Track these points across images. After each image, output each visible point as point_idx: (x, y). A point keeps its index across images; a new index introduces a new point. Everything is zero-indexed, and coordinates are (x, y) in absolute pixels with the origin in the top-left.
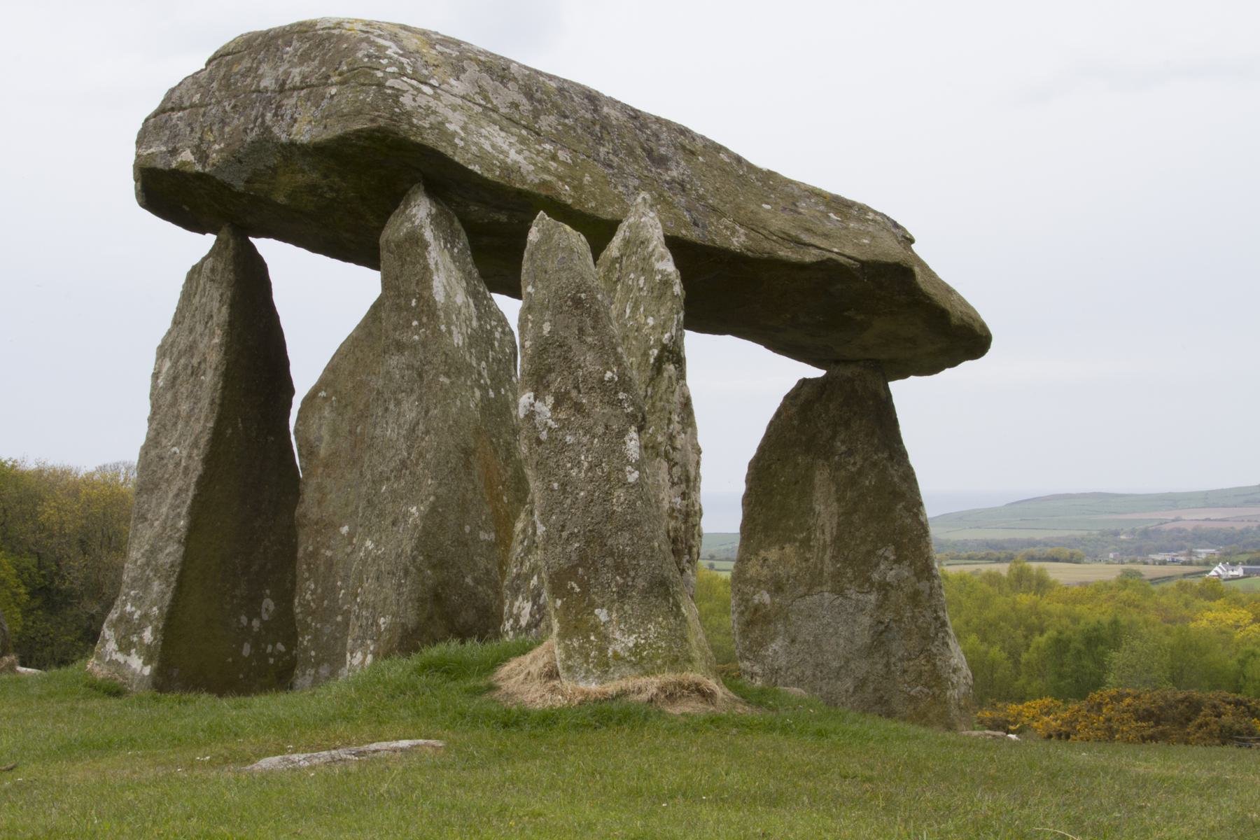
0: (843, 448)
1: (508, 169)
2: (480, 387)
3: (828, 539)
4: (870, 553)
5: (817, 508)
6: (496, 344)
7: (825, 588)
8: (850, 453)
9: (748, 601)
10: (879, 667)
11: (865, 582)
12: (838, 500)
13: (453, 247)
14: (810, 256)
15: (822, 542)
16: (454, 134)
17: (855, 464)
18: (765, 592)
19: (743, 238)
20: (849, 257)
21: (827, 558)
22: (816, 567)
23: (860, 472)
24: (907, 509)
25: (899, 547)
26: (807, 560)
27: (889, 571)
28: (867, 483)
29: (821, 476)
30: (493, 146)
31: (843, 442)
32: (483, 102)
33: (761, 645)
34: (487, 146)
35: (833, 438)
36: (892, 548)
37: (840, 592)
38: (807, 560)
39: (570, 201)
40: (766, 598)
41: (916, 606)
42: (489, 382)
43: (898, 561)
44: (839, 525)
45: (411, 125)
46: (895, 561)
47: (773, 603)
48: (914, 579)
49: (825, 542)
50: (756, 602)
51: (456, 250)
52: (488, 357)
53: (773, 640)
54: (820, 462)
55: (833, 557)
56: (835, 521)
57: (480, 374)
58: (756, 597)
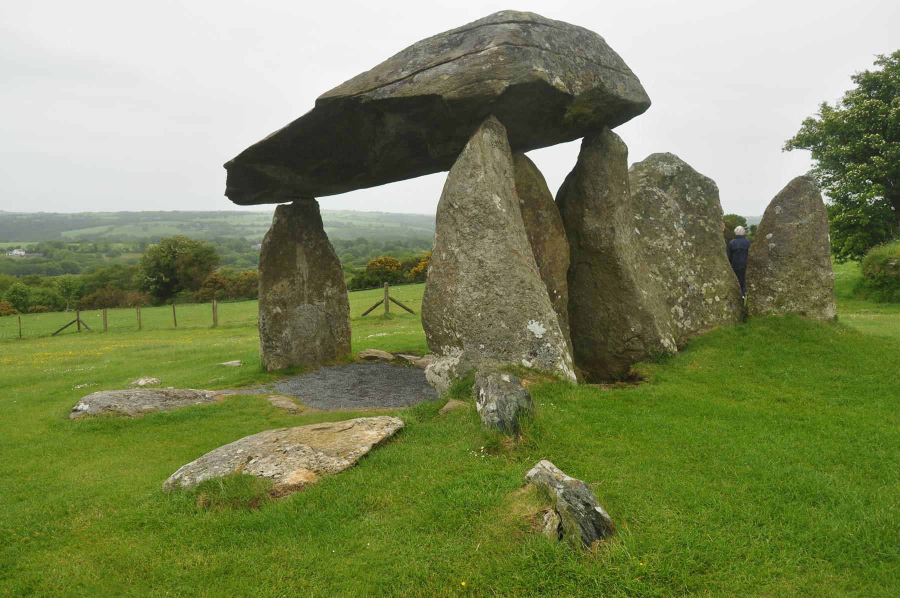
0: (306, 238)
3: (306, 280)
4: (324, 284)
5: (298, 266)
7: (305, 302)
8: (309, 240)
9: (270, 313)
10: (328, 332)
11: (321, 297)
12: (308, 261)
15: (301, 281)
17: (312, 245)
18: (278, 308)
21: (305, 288)
22: (300, 293)
23: (314, 248)
24: (336, 263)
25: (333, 280)
26: (295, 290)
27: (329, 291)
28: (318, 253)
29: (300, 250)
31: (306, 235)
33: (281, 333)
35: (301, 233)
36: (330, 281)
37: (311, 302)
38: (295, 290)
40: (279, 310)
41: (340, 304)
43: (332, 286)
44: (309, 272)
46: (332, 287)
47: (283, 312)
48: (339, 293)
49: (303, 280)
50: (275, 312)
53: (285, 330)
54: (298, 244)
55: (308, 287)
56: (307, 271)
58: (274, 310)
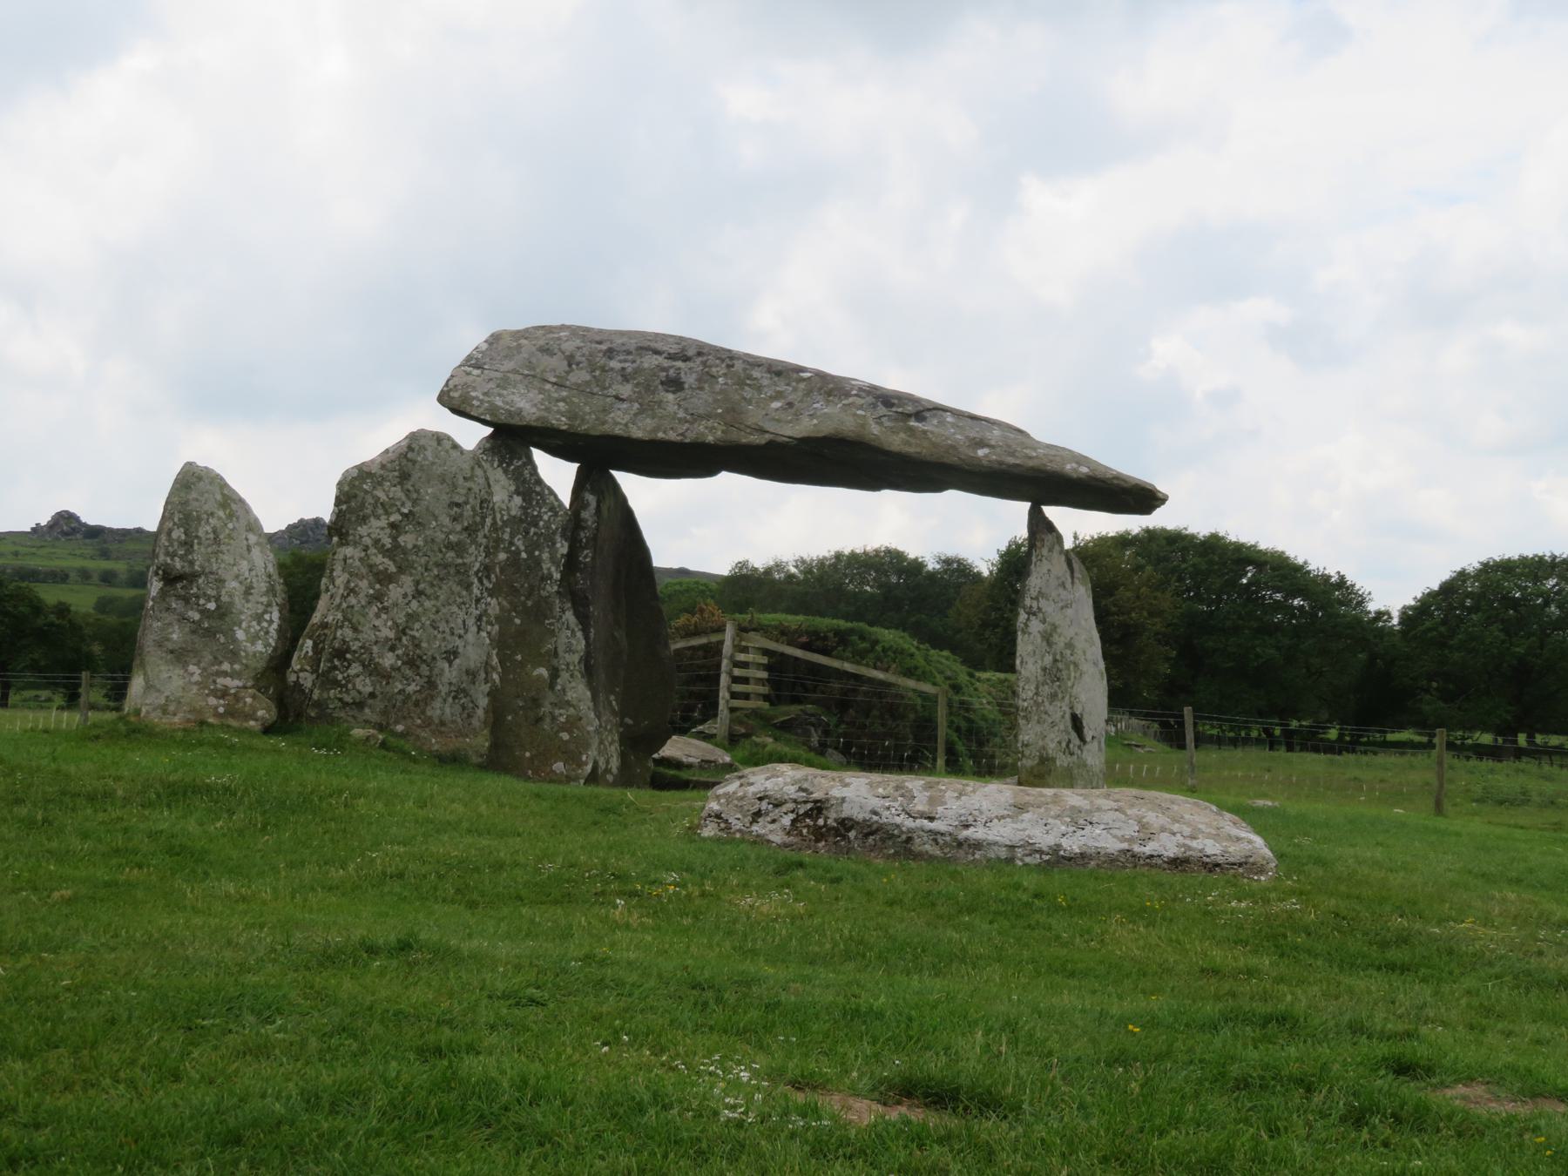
1: (509, 412)
2: (507, 550)
6: (541, 523)
13: (509, 465)
14: (768, 437)
16: (474, 398)
19: (719, 433)
20: (789, 437)
30: (503, 402)
32: (526, 372)
34: (499, 402)
39: (564, 428)
42: (522, 548)
45: (449, 396)
51: (512, 467)
52: (527, 533)
57: (511, 543)
